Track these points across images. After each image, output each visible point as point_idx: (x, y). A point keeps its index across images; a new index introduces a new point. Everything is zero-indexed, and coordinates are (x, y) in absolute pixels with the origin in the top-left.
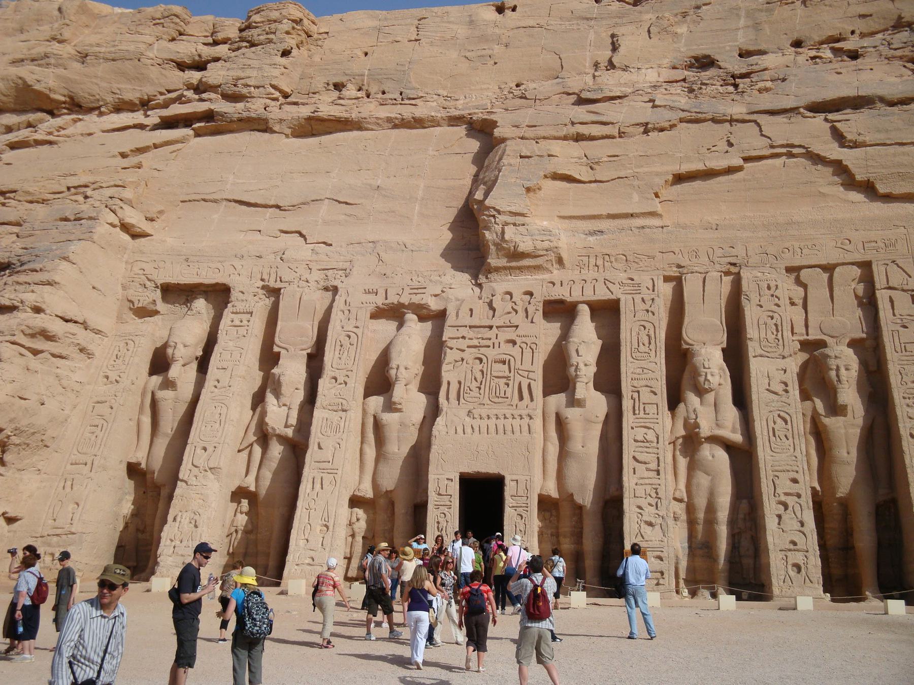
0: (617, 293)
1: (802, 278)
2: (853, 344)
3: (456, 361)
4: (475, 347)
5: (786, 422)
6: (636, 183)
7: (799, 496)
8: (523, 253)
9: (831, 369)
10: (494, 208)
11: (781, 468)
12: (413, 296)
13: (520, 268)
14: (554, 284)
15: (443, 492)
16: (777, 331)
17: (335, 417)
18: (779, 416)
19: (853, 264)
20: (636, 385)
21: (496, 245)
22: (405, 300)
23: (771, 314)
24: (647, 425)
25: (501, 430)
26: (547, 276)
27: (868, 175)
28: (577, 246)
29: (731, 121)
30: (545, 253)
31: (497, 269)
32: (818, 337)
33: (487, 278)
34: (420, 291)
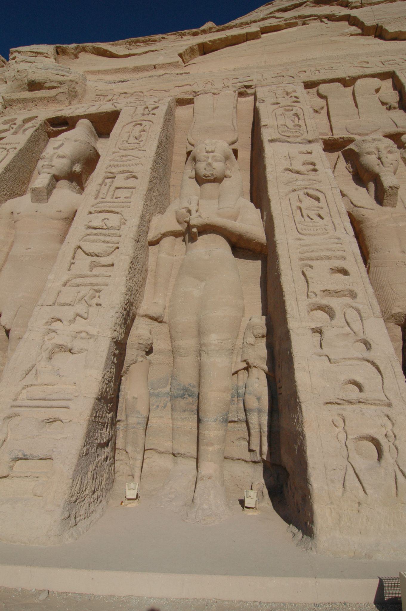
1: (320, 92)
5: (318, 199)
7: (353, 295)
8: (33, 81)
9: (369, 153)
11: (316, 254)
16: (299, 119)
18: (308, 194)
19: (373, 76)
20: (113, 171)
23: (290, 108)
24: (113, 209)
27: (376, 21)
28: (97, 88)
30: (59, 85)
32: (346, 135)
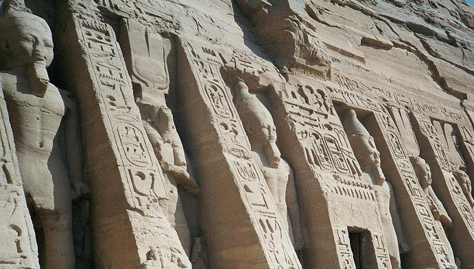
0: (369, 109)
2: (461, 168)
3: (302, 133)
4: (309, 124)
6: (347, 35)
10: (297, 15)
12: (246, 67)
13: (311, 71)
14: (331, 91)
15: (342, 242)
17: (244, 162)
19: (449, 123)
21: (301, 46)
22: (241, 68)
25: (360, 197)
26: (323, 82)
29: (372, 15)
31: (298, 66)
33: (289, 70)
34: (247, 64)
